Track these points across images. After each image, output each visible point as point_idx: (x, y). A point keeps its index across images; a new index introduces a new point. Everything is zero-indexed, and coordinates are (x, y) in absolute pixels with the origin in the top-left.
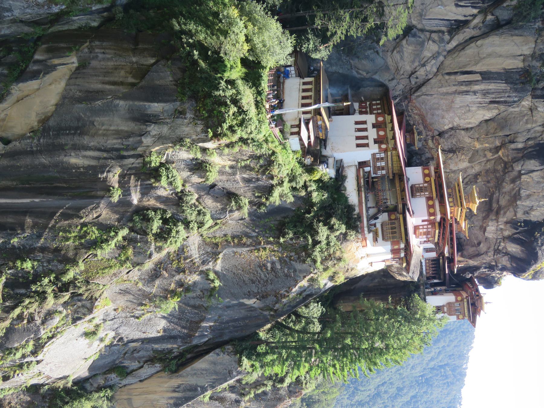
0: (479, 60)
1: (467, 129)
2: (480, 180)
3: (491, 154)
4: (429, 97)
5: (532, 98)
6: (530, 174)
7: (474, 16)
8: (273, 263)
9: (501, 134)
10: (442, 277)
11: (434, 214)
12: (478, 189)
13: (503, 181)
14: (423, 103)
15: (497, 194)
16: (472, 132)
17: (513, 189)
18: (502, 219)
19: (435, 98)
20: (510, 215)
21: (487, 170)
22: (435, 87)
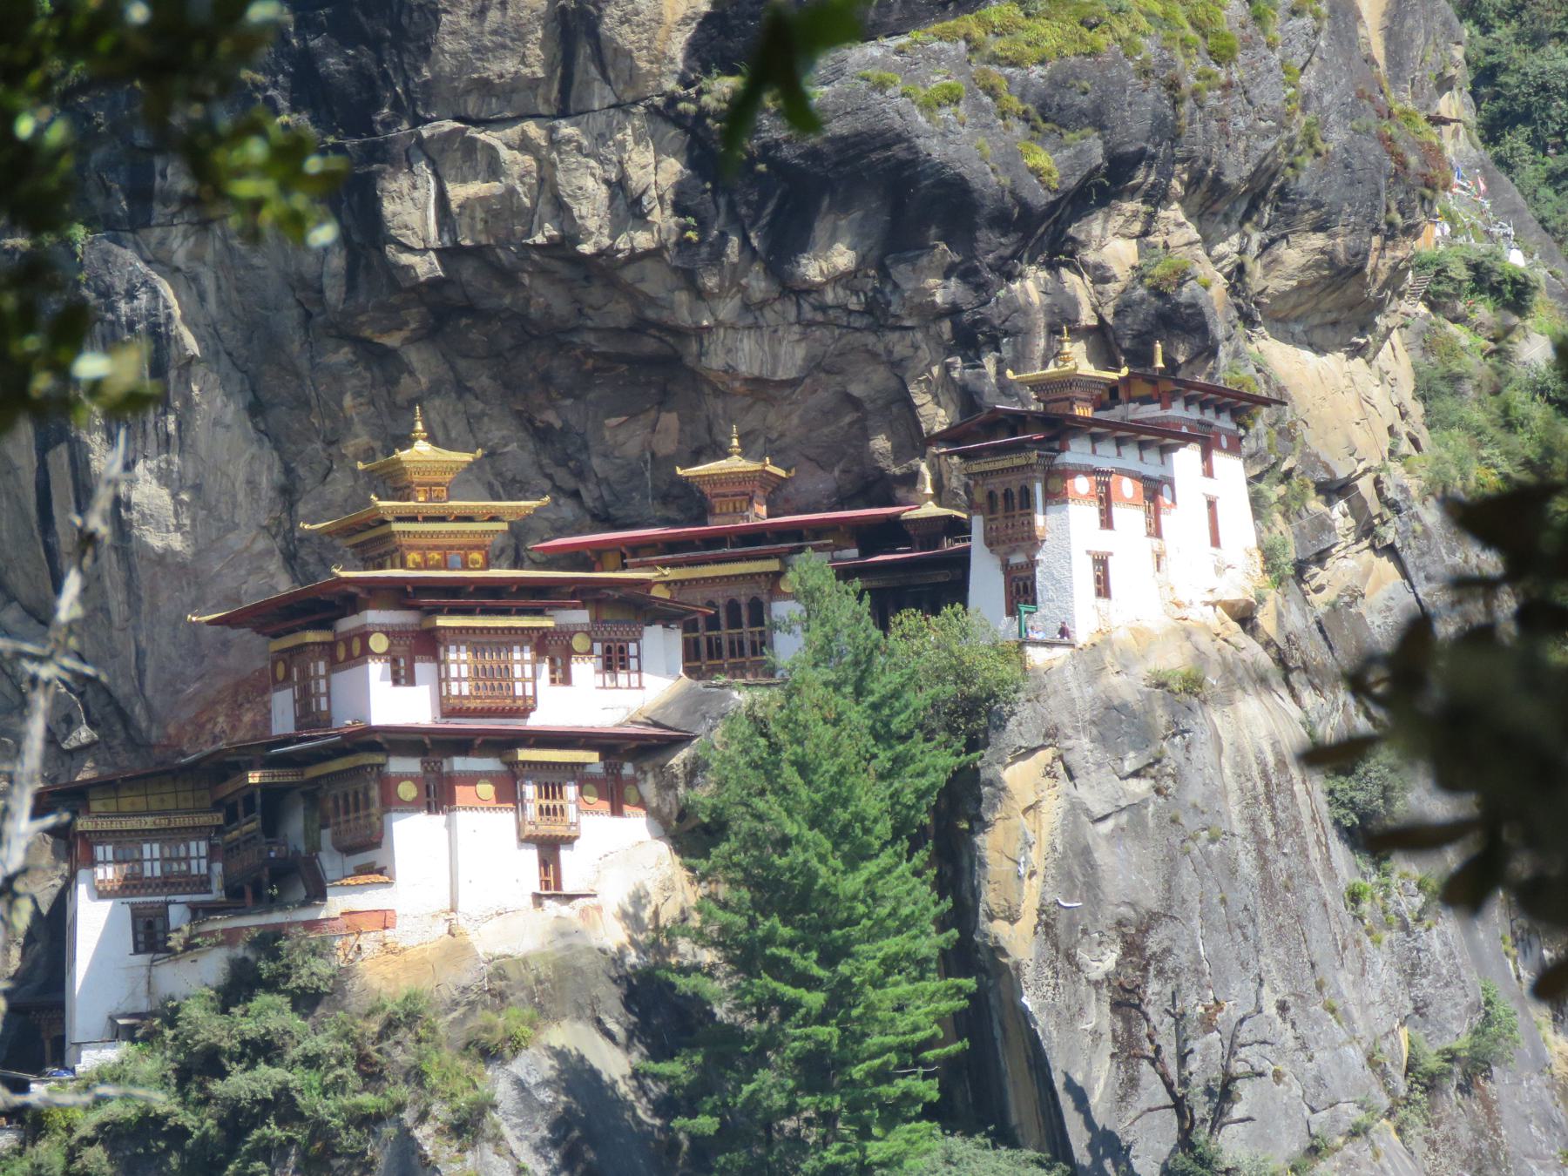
1: (288, 493)
2: (550, 417)
3: (405, 379)
4: (150, 664)
5: (147, 225)
6: (454, 206)
9: (296, 347)
10: (941, 577)
11: (364, 635)
12: (614, 421)
13: (519, 318)
14: (178, 692)
15: (590, 338)
16: (301, 471)
17: (543, 271)
18: (683, 309)
19: (151, 639)
20: (654, 282)
21: (506, 385)
22: (110, 638)
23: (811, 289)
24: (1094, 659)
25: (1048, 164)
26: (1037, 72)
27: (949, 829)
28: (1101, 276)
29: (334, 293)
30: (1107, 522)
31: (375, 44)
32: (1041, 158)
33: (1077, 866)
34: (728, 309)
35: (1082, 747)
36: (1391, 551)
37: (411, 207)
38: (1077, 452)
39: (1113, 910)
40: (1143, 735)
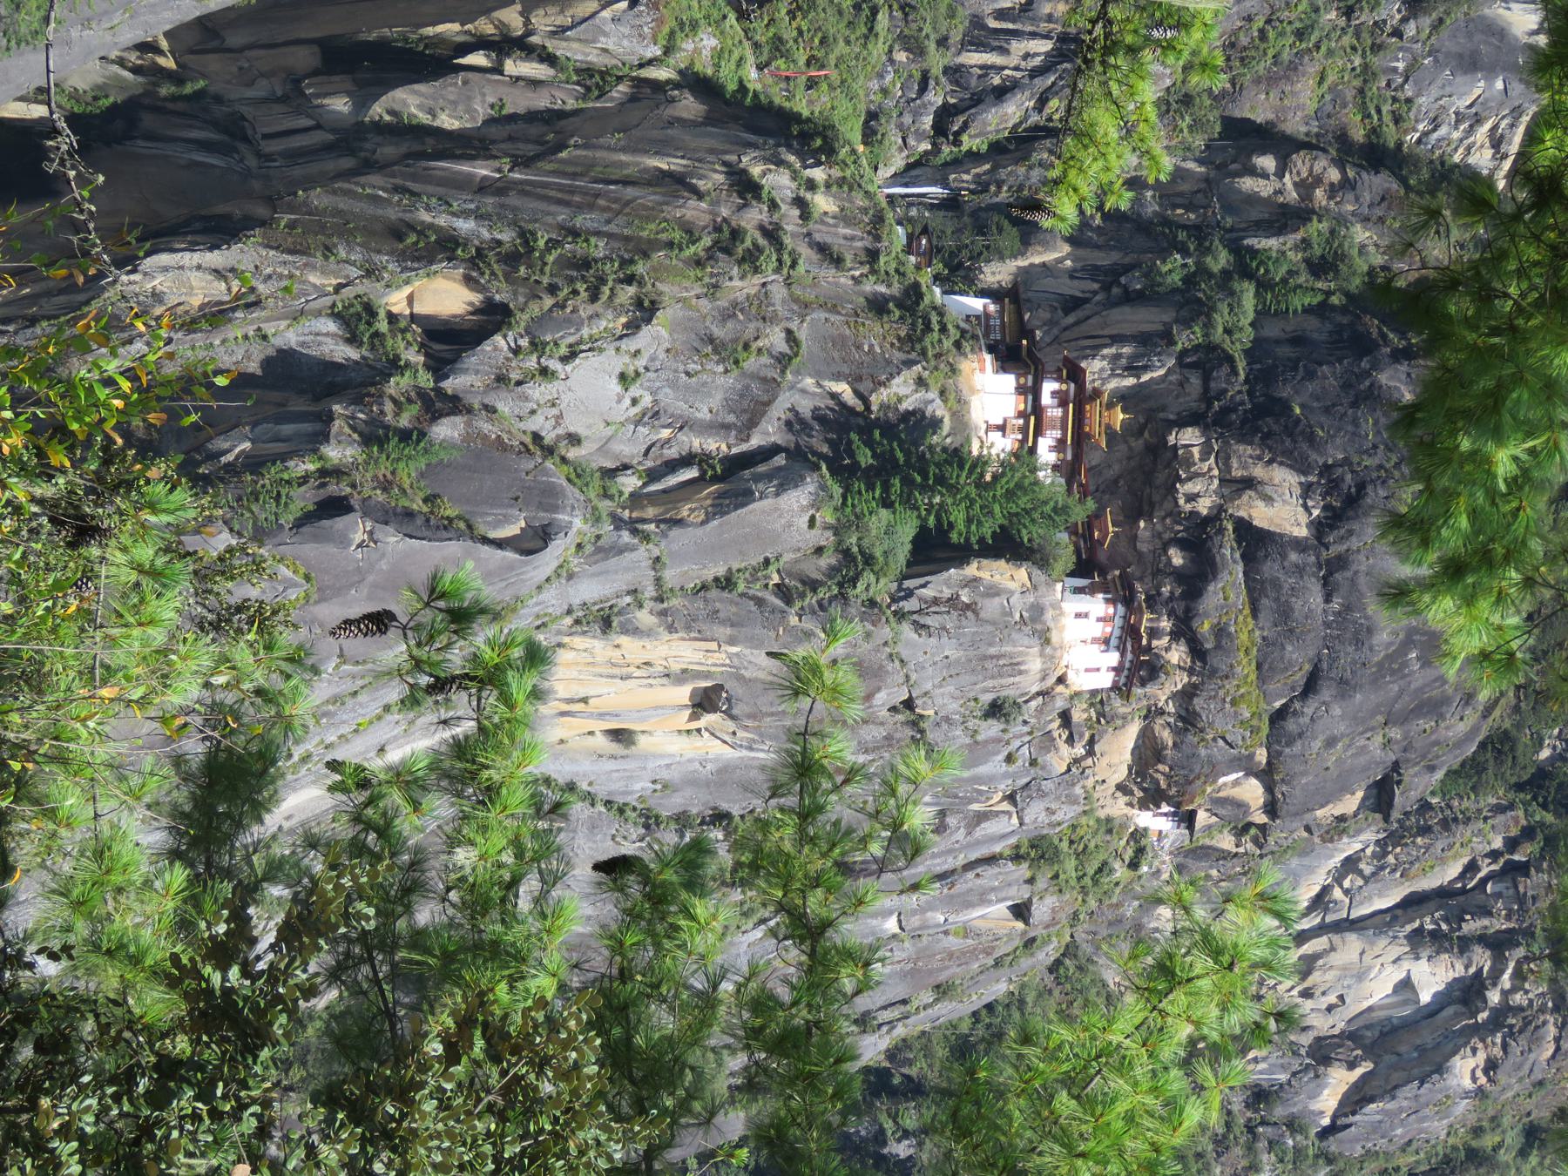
0: (1106, 325)
2: (1122, 483)
7: (1095, 293)
8: (871, 346)
17: (1170, 475)
18: (1159, 513)
20: (1168, 505)
23: (1165, 551)
24: (1056, 606)
25: (1205, 627)
26: (1232, 629)
27: (1007, 546)
28: (1167, 649)
29: (1161, 415)
30: (1099, 620)
31: (1241, 428)
32: (1206, 626)
33: (994, 591)
34: (1159, 527)
35: (1031, 599)
36: (1069, 770)
37: (1190, 437)
38: (1121, 609)
39: (979, 600)
40: (1034, 620)
